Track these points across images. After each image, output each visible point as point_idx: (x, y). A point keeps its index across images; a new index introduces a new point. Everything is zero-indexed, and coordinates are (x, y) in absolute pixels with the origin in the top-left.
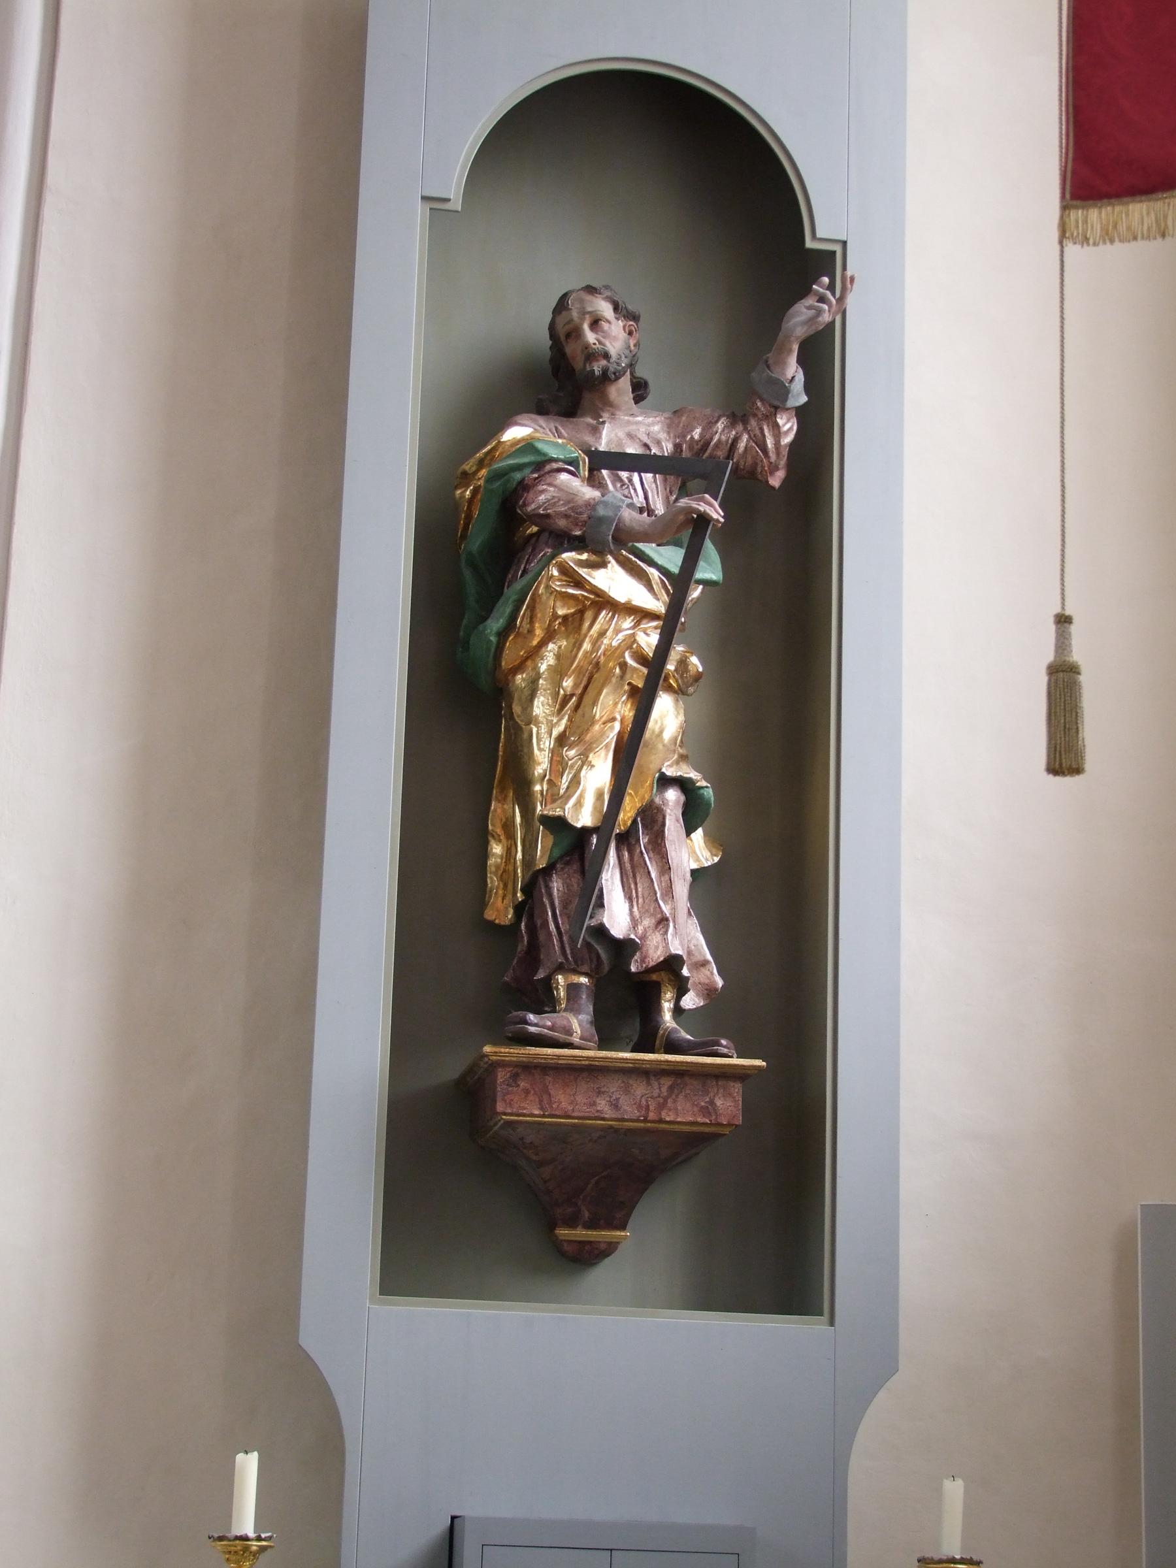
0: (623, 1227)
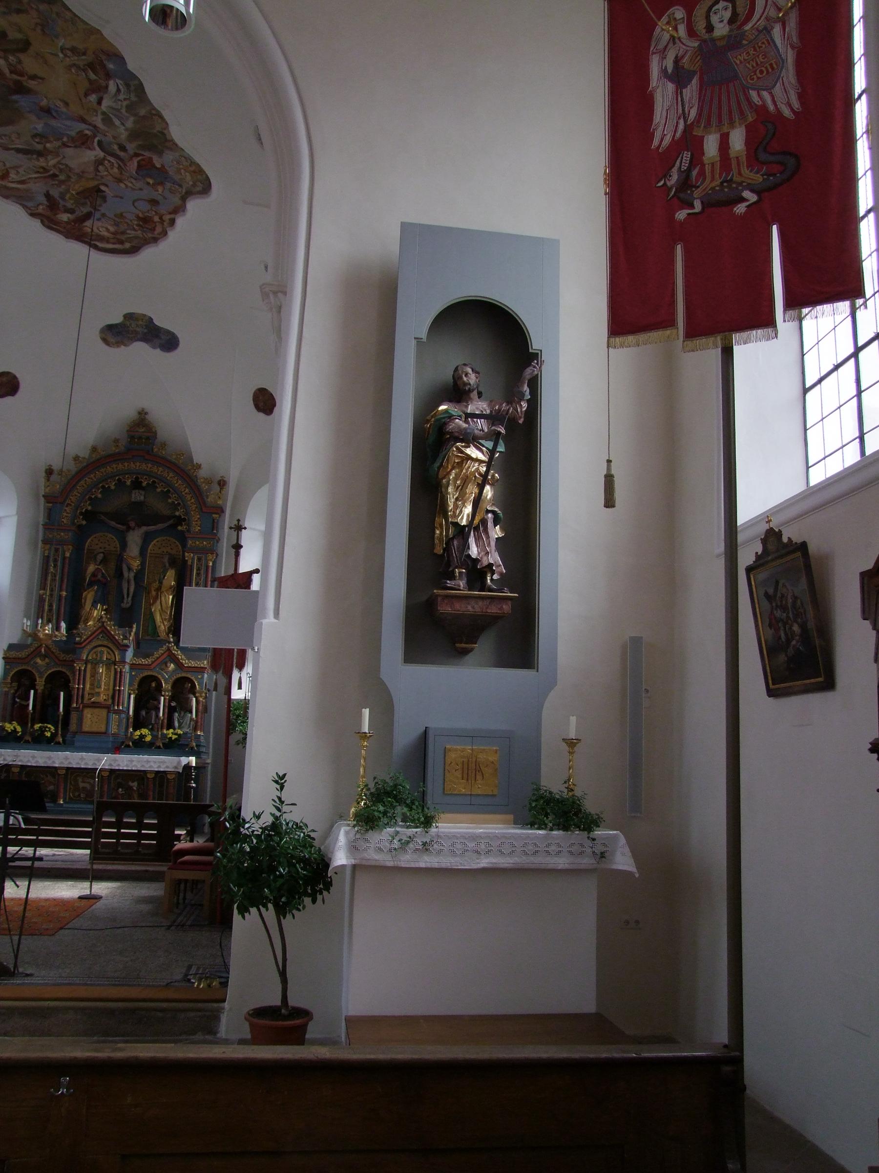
0: (476, 644)
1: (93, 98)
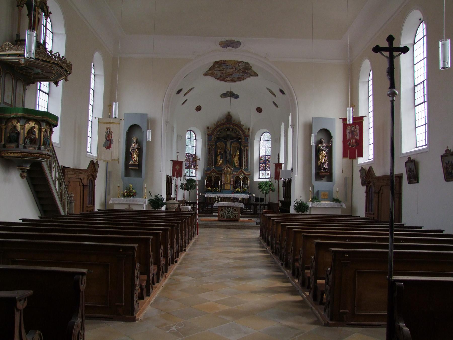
1: (238, 64)
